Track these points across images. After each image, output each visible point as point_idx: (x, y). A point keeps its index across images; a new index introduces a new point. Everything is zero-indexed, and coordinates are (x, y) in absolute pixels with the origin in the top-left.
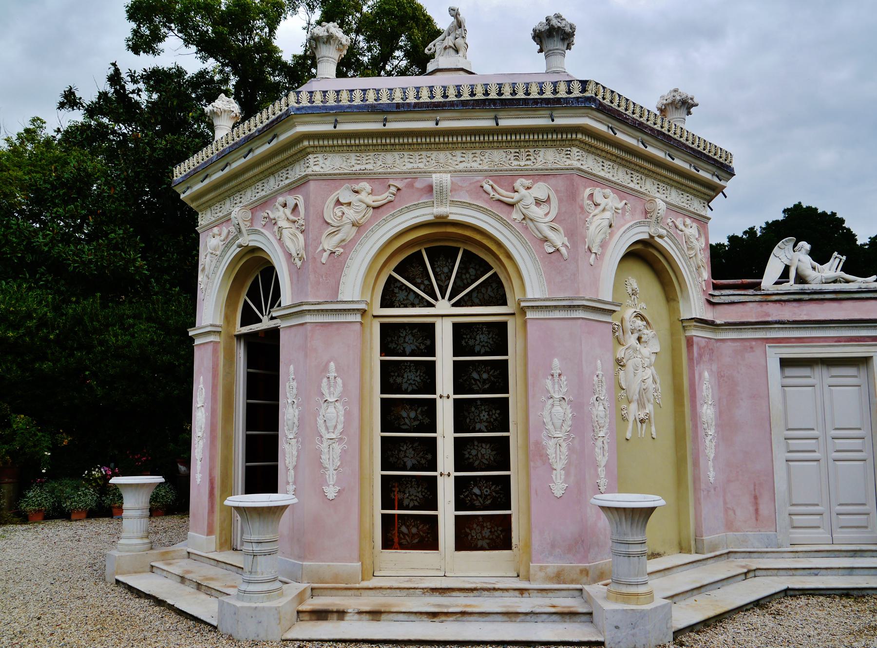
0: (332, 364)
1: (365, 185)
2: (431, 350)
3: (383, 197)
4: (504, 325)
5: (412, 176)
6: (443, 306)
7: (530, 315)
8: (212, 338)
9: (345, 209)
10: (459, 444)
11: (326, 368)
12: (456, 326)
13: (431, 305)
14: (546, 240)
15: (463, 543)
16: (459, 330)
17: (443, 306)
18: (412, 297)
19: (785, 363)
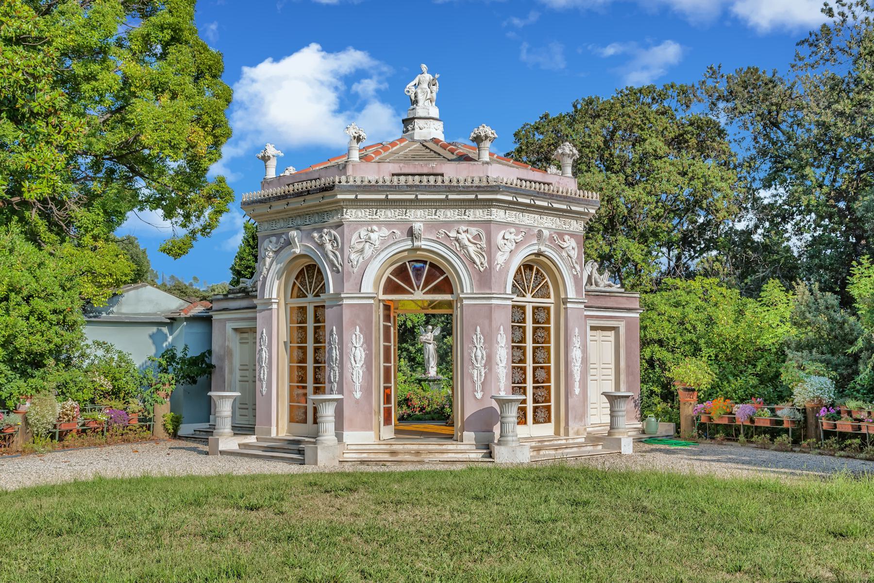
0: (502, 327)
1: (513, 230)
2: (524, 321)
3: (519, 238)
4: (548, 309)
5: (530, 228)
6: (529, 297)
7: (569, 305)
8: (372, 301)
9: (506, 241)
10: (535, 369)
11: (499, 330)
12: (534, 308)
13: (524, 296)
14: (574, 267)
15: (536, 421)
16: (536, 309)
17: (529, 297)
18: (517, 290)
19: (593, 328)
